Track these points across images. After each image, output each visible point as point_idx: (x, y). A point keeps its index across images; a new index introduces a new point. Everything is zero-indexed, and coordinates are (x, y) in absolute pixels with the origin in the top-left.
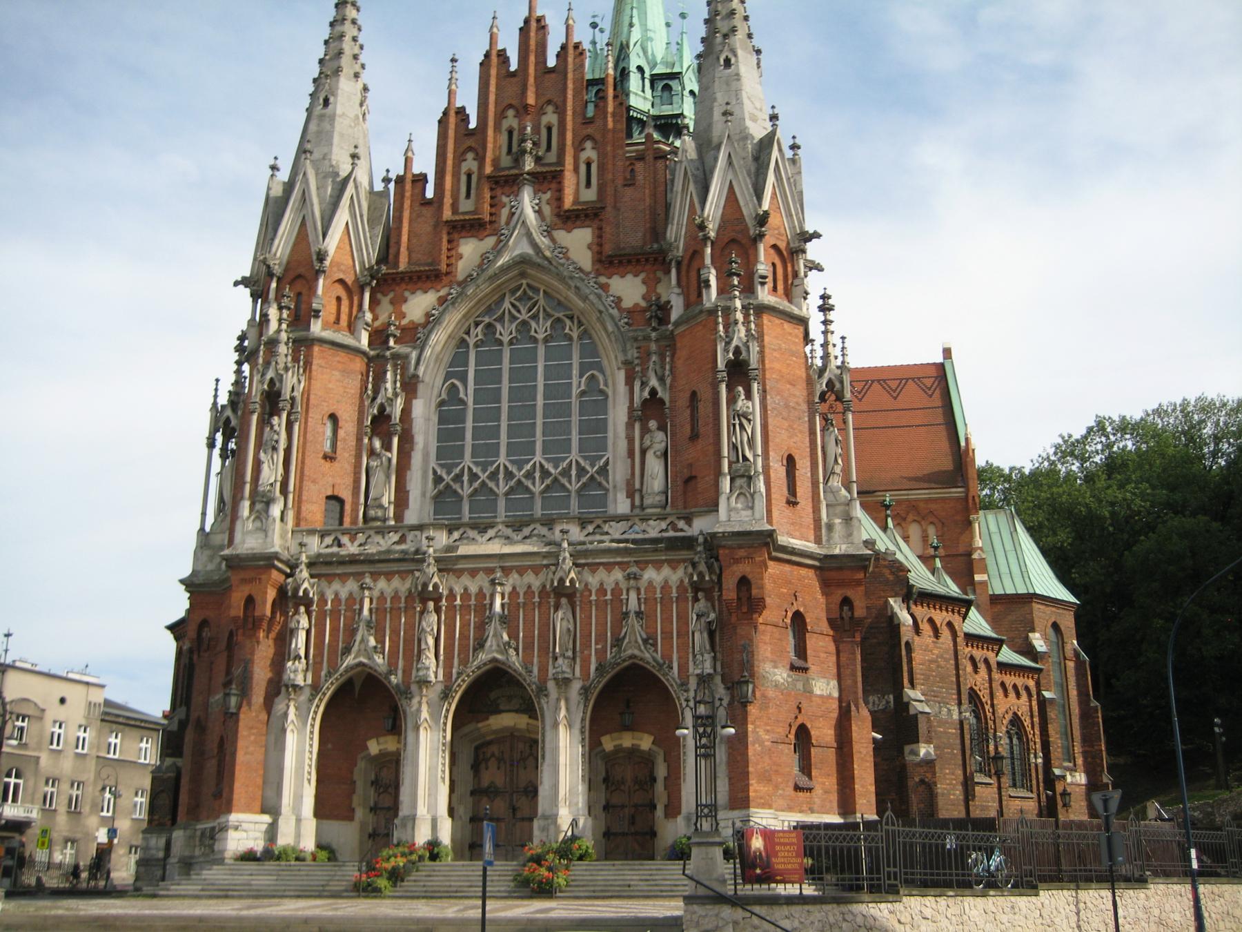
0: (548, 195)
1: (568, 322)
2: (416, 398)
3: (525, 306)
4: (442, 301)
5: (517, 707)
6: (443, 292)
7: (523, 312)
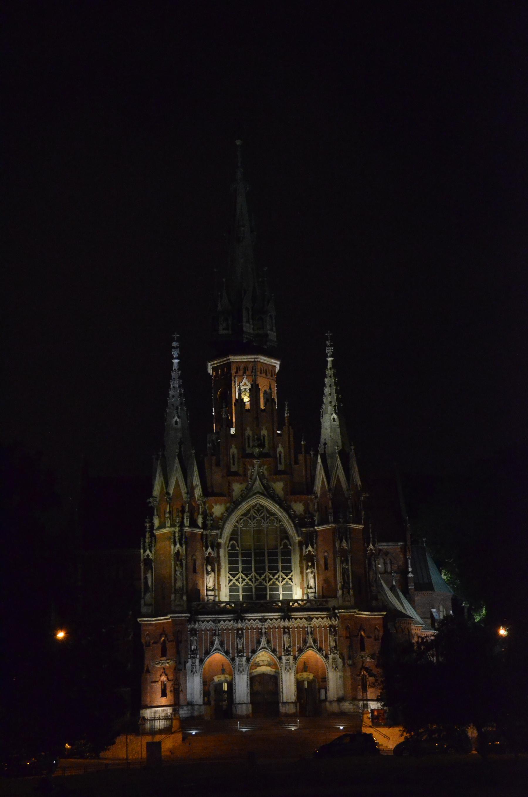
0: (265, 467)
1: (276, 521)
2: (221, 548)
3: (258, 512)
4: (227, 509)
5: (266, 664)
6: (228, 505)
7: (258, 515)
